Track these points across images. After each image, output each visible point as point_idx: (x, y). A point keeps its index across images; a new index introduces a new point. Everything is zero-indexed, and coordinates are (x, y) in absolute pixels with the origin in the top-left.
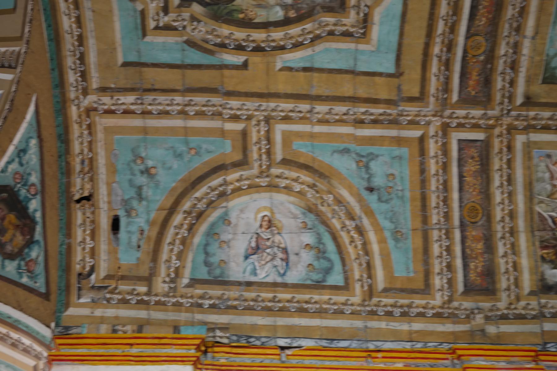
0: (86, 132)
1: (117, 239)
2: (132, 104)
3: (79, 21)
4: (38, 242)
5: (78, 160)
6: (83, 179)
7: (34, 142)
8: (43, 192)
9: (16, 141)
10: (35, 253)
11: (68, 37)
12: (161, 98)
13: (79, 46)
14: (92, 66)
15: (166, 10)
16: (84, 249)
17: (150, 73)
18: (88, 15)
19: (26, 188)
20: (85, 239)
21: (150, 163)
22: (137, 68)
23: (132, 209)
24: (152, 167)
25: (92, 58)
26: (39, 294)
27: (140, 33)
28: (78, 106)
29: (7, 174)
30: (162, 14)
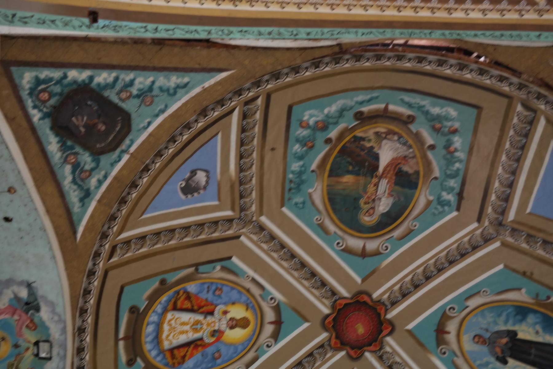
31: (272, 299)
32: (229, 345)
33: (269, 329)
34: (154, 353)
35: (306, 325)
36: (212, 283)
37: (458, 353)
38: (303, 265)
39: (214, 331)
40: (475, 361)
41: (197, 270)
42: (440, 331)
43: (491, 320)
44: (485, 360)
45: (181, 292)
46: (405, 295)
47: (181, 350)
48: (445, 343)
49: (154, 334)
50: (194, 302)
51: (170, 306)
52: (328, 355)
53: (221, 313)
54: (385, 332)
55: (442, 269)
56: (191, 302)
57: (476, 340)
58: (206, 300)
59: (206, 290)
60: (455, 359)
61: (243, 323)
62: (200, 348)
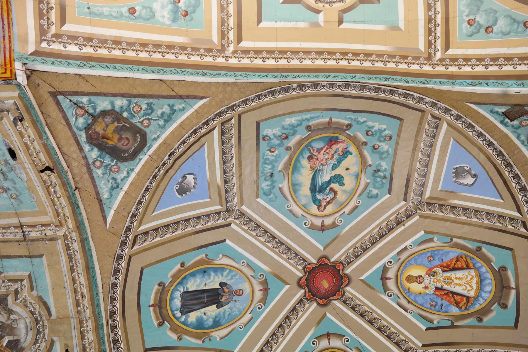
0: (60, 211)
1: (6, 145)
2: (31, 231)
3: (74, 282)
4: (81, 130)
5: (59, 193)
6: (51, 181)
7: (105, 195)
8: (88, 165)
9: (122, 193)
10: (81, 121)
11: (81, 270)
12: (11, 237)
13: (73, 266)
14: (63, 254)
15: (16, 292)
16: (29, 137)
17: (23, 251)
18: (68, 285)
19: (104, 164)
20: (32, 143)
21: (5, 195)
22: (31, 254)
23: (5, 165)
24: (3, 193)
25: (64, 259)
26: (64, 94)
27: (33, 277)
28: (68, 228)
29: (126, 169)
30: (19, 289)
31: (391, 296)
32: (422, 265)
33: (391, 274)
34: (483, 270)
35: (362, 278)
36: (439, 311)
37: (251, 278)
38: (371, 322)
39: (434, 276)
40: (240, 277)
41: (453, 323)
42: (265, 290)
43: (234, 309)
44: (234, 280)
45: (463, 308)
46: (294, 309)
47: (460, 266)
48: (261, 283)
49: (484, 283)
50: (453, 299)
51: (471, 301)
52: (343, 257)
53: (429, 286)
54: (303, 280)
55: (272, 336)
56: (454, 300)
57: (241, 291)
58: (442, 299)
59: (443, 307)
60: (253, 274)
61: (410, 279)
62: (445, 265)
